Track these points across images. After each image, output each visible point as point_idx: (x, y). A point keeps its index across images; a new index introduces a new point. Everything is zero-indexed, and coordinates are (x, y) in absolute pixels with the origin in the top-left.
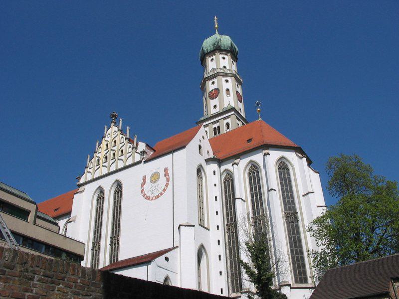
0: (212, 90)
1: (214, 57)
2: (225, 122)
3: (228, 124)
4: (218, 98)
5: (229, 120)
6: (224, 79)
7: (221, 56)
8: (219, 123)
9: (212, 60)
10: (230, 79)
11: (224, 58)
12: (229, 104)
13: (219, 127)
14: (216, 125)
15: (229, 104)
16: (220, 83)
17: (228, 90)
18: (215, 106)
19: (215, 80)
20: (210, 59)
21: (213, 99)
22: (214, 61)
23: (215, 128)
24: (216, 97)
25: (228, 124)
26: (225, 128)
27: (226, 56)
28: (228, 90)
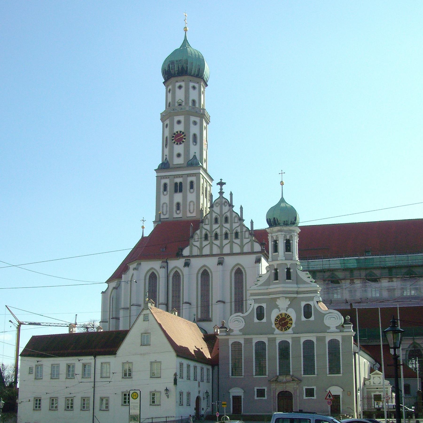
0: (177, 132)
1: (183, 84)
2: (190, 179)
3: (192, 183)
4: (182, 146)
5: (194, 179)
6: (192, 119)
7: (191, 84)
9: (180, 87)
10: (197, 120)
11: (194, 88)
12: (195, 156)
13: (181, 183)
14: (178, 180)
15: (195, 156)
16: (187, 126)
17: (195, 135)
18: (179, 155)
20: (178, 84)
21: (177, 144)
22: (183, 89)
23: (176, 184)
24: (180, 144)
25: (192, 183)
26: (188, 187)
27: (197, 85)
28: (195, 135)
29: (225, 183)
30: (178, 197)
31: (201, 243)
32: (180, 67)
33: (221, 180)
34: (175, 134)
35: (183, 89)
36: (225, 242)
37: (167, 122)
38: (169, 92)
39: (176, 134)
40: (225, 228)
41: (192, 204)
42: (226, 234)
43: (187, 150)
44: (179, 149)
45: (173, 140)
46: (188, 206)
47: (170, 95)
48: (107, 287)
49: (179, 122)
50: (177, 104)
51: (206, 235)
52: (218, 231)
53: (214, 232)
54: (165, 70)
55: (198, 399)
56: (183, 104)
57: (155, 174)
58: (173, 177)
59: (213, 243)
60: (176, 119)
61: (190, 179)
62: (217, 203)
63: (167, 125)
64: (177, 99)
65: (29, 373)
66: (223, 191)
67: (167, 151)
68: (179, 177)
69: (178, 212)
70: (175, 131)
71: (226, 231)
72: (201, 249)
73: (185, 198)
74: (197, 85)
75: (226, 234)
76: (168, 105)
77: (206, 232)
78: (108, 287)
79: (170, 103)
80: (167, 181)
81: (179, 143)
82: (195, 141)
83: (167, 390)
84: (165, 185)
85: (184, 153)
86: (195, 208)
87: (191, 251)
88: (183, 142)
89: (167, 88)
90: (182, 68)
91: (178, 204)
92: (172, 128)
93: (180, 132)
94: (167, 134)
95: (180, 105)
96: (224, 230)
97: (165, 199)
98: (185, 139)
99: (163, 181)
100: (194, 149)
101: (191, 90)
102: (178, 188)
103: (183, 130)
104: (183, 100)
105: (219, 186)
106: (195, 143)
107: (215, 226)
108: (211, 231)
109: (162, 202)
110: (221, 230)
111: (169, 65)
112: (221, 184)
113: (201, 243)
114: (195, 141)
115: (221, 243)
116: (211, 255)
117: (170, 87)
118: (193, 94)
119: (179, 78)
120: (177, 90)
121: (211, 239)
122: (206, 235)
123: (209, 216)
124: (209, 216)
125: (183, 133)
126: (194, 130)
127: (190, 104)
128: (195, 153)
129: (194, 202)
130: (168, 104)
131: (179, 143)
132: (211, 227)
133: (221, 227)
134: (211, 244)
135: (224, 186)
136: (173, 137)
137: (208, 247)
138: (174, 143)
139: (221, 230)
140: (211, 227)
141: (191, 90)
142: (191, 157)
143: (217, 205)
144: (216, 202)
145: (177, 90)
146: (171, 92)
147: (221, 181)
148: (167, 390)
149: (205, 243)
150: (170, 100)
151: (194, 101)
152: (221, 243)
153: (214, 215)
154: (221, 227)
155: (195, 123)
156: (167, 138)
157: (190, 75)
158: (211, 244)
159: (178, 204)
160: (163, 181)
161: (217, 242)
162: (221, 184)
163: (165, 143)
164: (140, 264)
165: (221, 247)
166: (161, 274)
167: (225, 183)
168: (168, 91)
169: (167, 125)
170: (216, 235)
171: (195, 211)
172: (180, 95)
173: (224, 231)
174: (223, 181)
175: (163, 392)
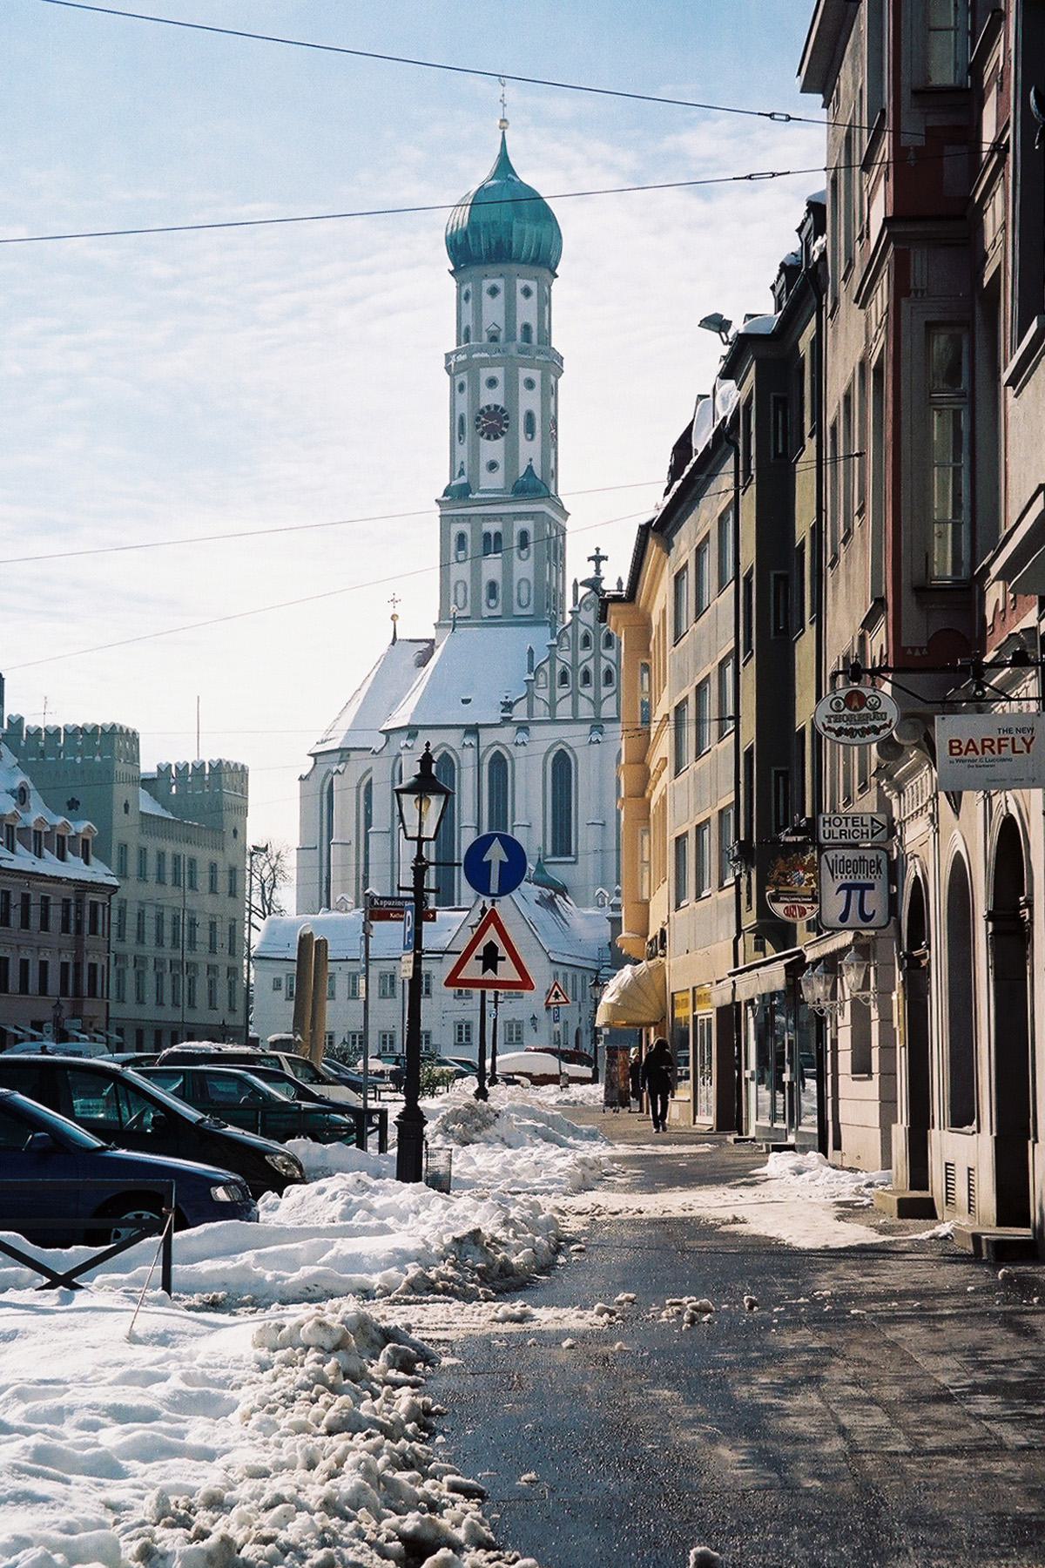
0: (488, 407)
2: (520, 525)
3: (524, 535)
4: (501, 442)
5: (528, 525)
7: (520, 283)
8: (500, 524)
9: (494, 291)
10: (535, 375)
11: (527, 292)
12: (530, 467)
13: (498, 535)
14: (492, 527)
15: (530, 467)
17: (530, 415)
18: (492, 466)
19: (498, 372)
20: (487, 284)
21: (488, 438)
22: (501, 297)
23: (487, 536)
24: (496, 438)
25: (524, 535)
26: (516, 543)
27: (533, 285)
28: (530, 415)
29: (605, 558)
30: (492, 568)
31: (552, 694)
32: (493, 243)
33: (598, 549)
34: (482, 412)
35: (501, 297)
36: (605, 691)
37: (463, 377)
38: (467, 298)
39: (486, 411)
40: (606, 658)
41: (524, 585)
42: (608, 674)
43: (512, 453)
44: (493, 449)
45: (478, 427)
46: (515, 594)
47: (468, 307)
48: (313, 763)
49: (492, 383)
50: (485, 337)
51: (564, 676)
52: (591, 665)
53: (582, 668)
54: (456, 241)
55: (578, 1032)
56: (502, 336)
57: (436, 511)
58: (480, 518)
59: (579, 692)
60: (486, 374)
61: (520, 525)
62: (587, 602)
63: (461, 387)
64: (486, 325)
65: (274, 989)
66: (602, 574)
67: (463, 452)
68: (495, 520)
69: (492, 603)
70: (483, 404)
71: (608, 666)
72: (552, 705)
73: (507, 570)
74: (533, 285)
75: (608, 674)
76: (464, 335)
77: (564, 667)
78: (315, 763)
79: (467, 329)
80: (465, 527)
81: (492, 437)
82: (530, 429)
83: (534, 1018)
84: (461, 537)
85: (506, 460)
86: (532, 596)
87: (530, 711)
88: (503, 433)
89: (459, 288)
90: (499, 243)
91: (492, 586)
92: (475, 395)
93: (496, 407)
94: (463, 407)
95: (494, 339)
96: (604, 664)
97: (461, 572)
98: (507, 426)
99: (456, 528)
100: (529, 451)
101: (520, 296)
102: (492, 543)
103: (501, 404)
104: (502, 326)
105: (593, 563)
106: (529, 436)
107: (584, 655)
108: (575, 666)
109: (453, 580)
110: (597, 665)
111: (466, 233)
112: (598, 559)
113: (552, 694)
114: (530, 429)
115: (597, 692)
116: (575, 720)
117: (468, 287)
118: (526, 311)
119: (491, 269)
120: (486, 297)
121: (575, 684)
122: (564, 676)
123: (569, 631)
124: (569, 631)
125: (503, 411)
126: (529, 401)
127: (519, 335)
128: (531, 460)
129: (529, 583)
130: (463, 333)
131: (492, 437)
132: (575, 656)
133: (597, 656)
134: (575, 694)
135: (603, 563)
136: (478, 419)
137: (569, 701)
138: (482, 434)
139: (597, 665)
140: (575, 656)
141: (520, 296)
142: (522, 471)
143: (588, 606)
144: (586, 599)
145: (486, 297)
146: (471, 301)
147: (598, 552)
148: (534, 1018)
149: (560, 692)
150: (468, 321)
151: (527, 327)
152: (597, 692)
153: (582, 629)
154: (597, 656)
155: (530, 384)
156: (462, 419)
157: (517, 260)
158: (575, 694)
159: (492, 586)
160: (456, 528)
161: (588, 691)
162: (598, 559)
163: (459, 428)
164: (417, 733)
165: (597, 703)
166: (468, 757)
167: (605, 558)
168: (463, 298)
169: (461, 387)
170: (586, 677)
171: (532, 602)
172: (493, 311)
173: (603, 668)
174: (601, 553)
175: (527, 1023)
